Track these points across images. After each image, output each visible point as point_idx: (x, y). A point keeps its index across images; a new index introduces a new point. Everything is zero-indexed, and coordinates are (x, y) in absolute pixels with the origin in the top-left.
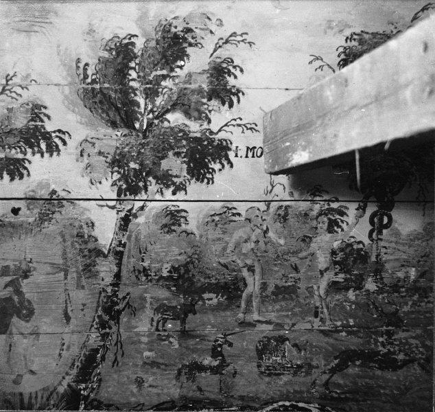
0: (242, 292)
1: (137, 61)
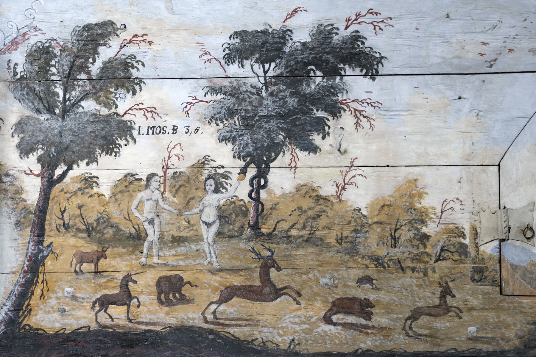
0: (145, 240)
1: (57, 60)
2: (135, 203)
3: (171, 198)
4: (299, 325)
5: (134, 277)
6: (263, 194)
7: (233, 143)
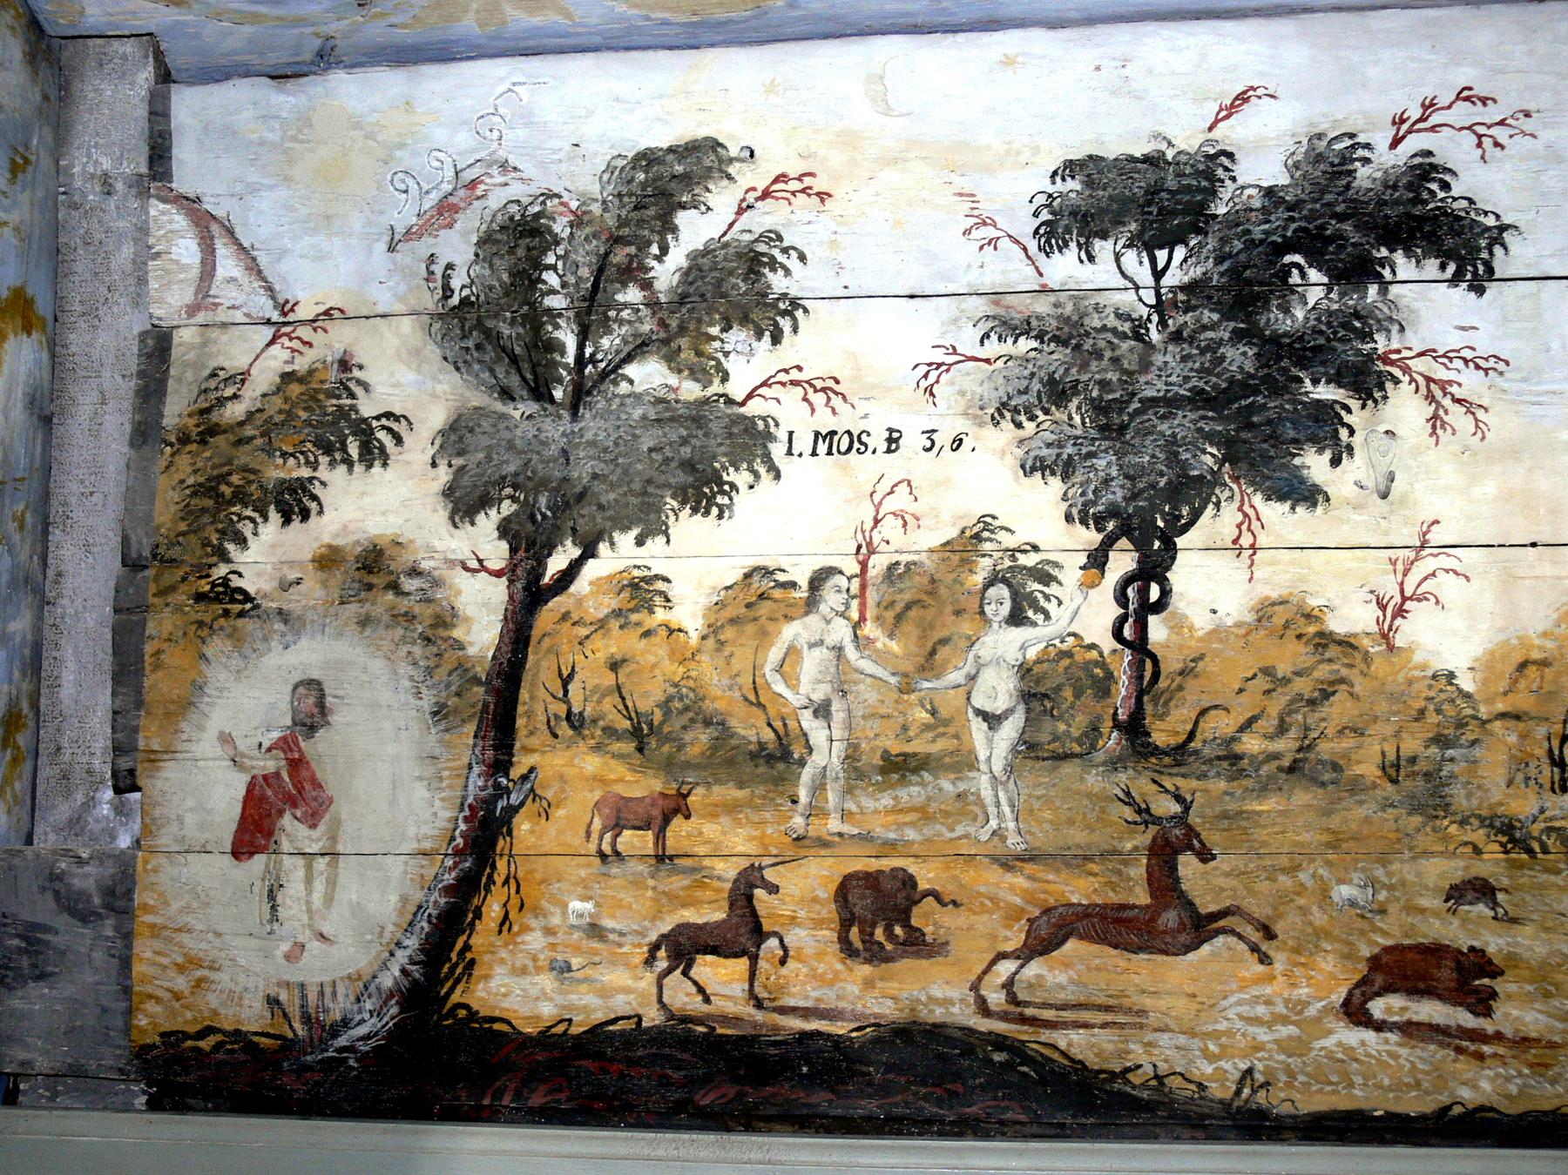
0: (802, 763)
1: (560, 251)
2: (775, 654)
3: (882, 641)
4: (1269, 1025)
5: (769, 875)
6: (1157, 629)
7: (1065, 477)
